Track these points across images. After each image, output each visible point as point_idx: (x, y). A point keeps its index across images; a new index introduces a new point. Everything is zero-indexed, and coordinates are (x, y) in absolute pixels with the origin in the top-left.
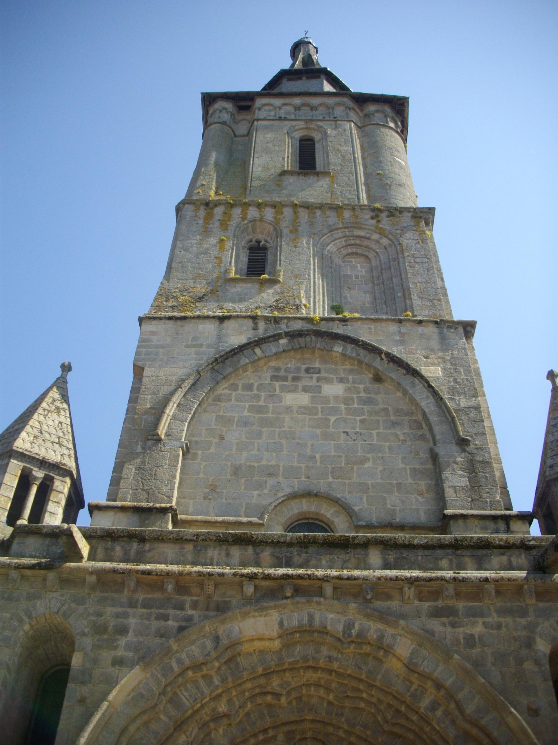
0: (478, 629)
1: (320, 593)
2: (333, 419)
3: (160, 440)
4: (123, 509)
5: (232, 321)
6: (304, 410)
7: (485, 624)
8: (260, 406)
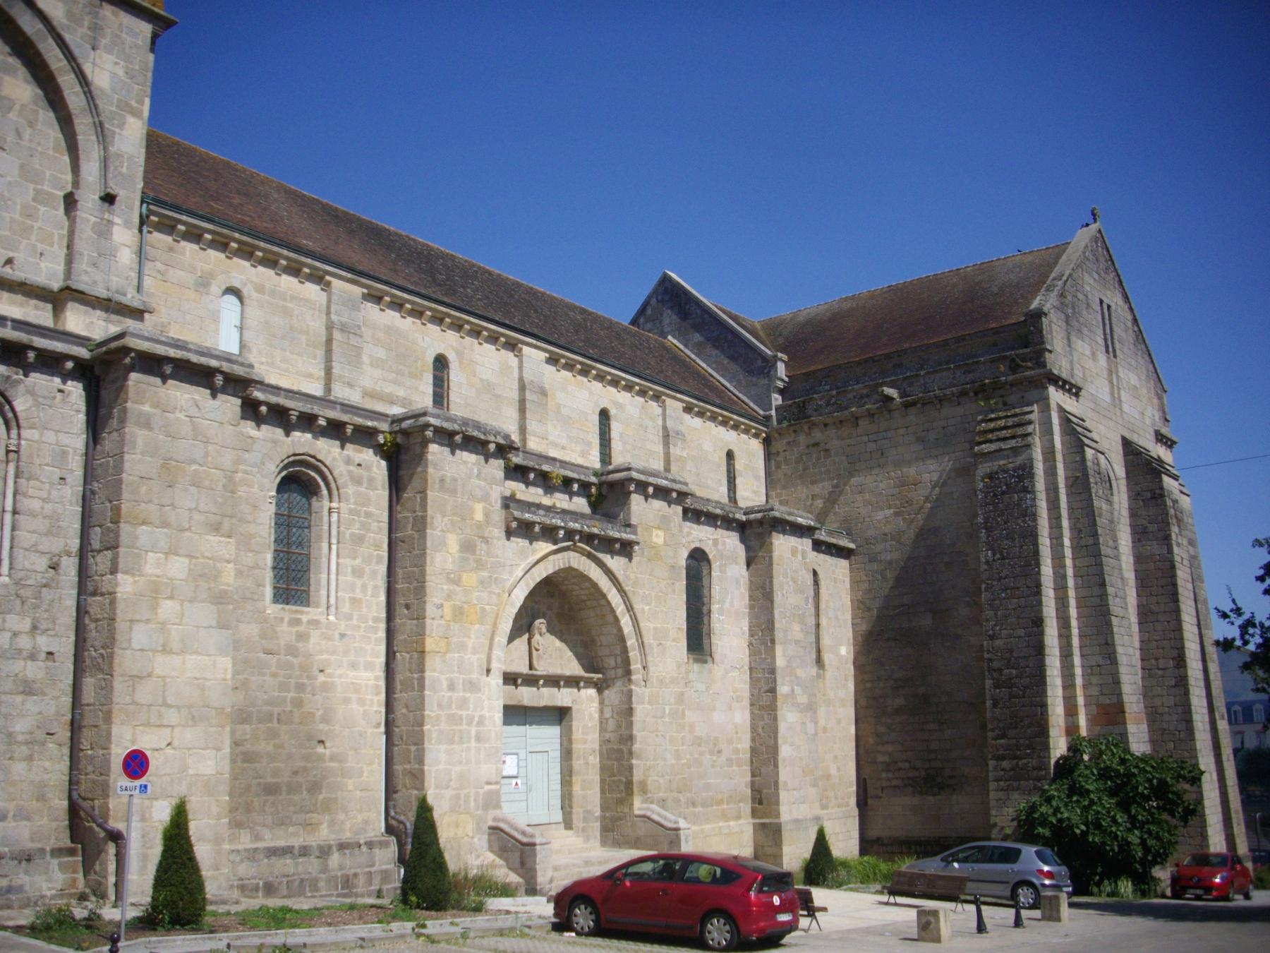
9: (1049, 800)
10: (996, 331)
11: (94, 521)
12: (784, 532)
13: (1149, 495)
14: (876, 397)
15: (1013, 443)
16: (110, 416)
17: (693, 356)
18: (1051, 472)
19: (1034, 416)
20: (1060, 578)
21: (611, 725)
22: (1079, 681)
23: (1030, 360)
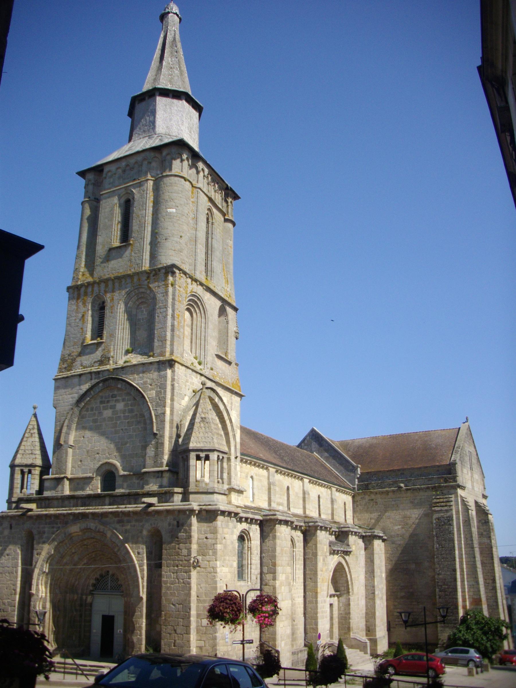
0: (128, 527)
1: (88, 518)
2: (118, 422)
3: (62, 445)
4: (52, 479)
5: (84, 376)
6: (111, 419)
7: (131, 526)
8: (96, 419)
9: (460, 631)
10: (438, 466)
11: (264, 564)
12: (376, 539)
13: (483, 521)
14: (396, 485)
15: (446, 508)
16: (268, 536)
17: (324, 462)
18: (458, 518)
19: (453, 499)
20: (461, 555)
21: (342, 608)
22: (466, 590)
23: (452, 479)
